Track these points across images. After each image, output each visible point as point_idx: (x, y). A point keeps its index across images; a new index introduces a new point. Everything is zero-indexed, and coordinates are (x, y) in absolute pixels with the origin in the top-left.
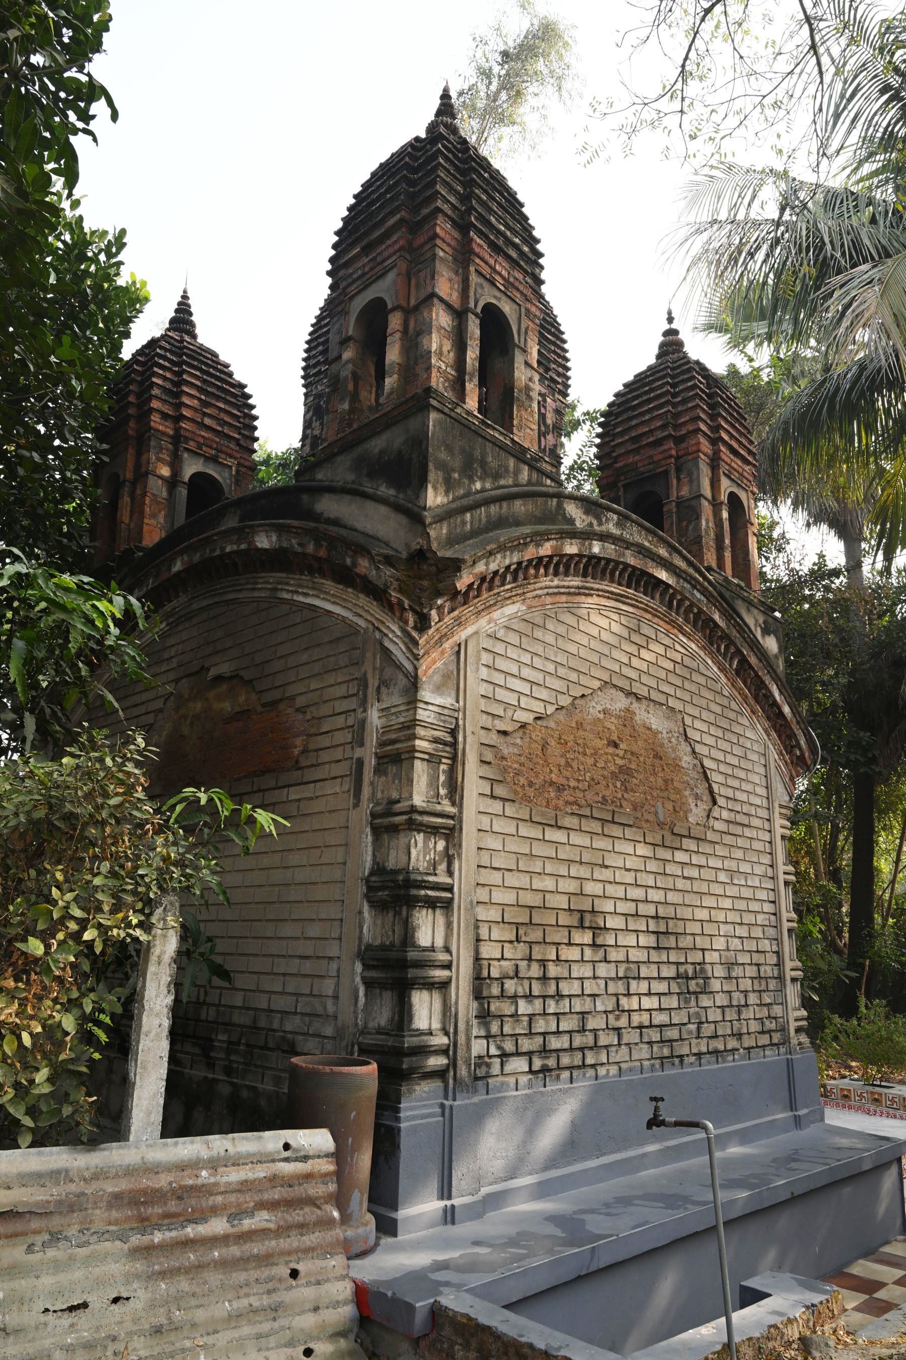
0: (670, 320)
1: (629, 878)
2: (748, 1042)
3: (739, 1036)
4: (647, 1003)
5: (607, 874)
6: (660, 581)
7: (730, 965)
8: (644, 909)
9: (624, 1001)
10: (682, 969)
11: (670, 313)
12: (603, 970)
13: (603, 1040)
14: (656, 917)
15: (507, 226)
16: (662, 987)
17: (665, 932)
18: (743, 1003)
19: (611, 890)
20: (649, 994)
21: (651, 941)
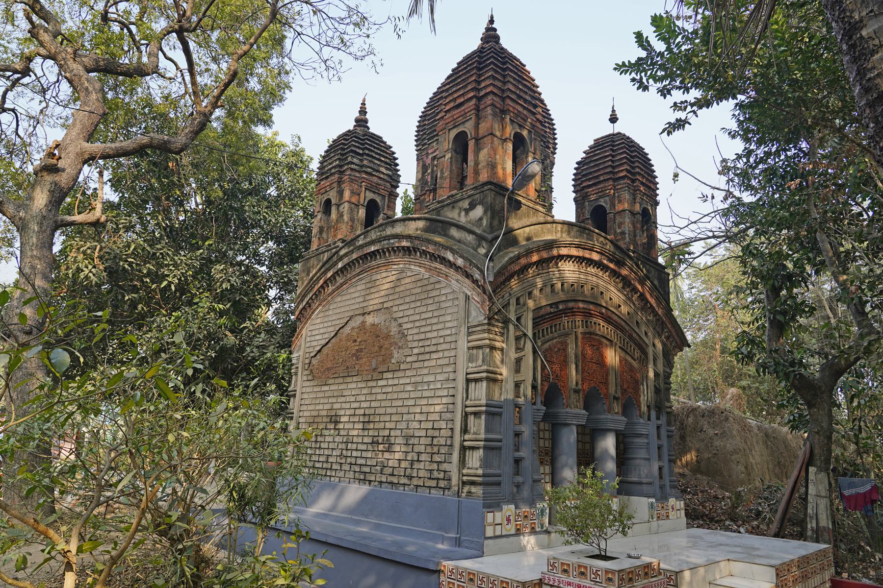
0: (492, 21)
1: (353, 399)
2: (415, 482)
3: (410, 478)
4: (355, 454)
5: (343, 399)
7: (407, 437)
8: (358, 412)
9: (344, 452)
10: (375, 439)
11: (492, 17)
12: (337, 439)
13: (334, 467)
14: (364, 415)
16: (364, 447)
17: (367, 421)
18: (416, 459)
19: (344, 405)
20: (356, 450)
21: (360, 426)
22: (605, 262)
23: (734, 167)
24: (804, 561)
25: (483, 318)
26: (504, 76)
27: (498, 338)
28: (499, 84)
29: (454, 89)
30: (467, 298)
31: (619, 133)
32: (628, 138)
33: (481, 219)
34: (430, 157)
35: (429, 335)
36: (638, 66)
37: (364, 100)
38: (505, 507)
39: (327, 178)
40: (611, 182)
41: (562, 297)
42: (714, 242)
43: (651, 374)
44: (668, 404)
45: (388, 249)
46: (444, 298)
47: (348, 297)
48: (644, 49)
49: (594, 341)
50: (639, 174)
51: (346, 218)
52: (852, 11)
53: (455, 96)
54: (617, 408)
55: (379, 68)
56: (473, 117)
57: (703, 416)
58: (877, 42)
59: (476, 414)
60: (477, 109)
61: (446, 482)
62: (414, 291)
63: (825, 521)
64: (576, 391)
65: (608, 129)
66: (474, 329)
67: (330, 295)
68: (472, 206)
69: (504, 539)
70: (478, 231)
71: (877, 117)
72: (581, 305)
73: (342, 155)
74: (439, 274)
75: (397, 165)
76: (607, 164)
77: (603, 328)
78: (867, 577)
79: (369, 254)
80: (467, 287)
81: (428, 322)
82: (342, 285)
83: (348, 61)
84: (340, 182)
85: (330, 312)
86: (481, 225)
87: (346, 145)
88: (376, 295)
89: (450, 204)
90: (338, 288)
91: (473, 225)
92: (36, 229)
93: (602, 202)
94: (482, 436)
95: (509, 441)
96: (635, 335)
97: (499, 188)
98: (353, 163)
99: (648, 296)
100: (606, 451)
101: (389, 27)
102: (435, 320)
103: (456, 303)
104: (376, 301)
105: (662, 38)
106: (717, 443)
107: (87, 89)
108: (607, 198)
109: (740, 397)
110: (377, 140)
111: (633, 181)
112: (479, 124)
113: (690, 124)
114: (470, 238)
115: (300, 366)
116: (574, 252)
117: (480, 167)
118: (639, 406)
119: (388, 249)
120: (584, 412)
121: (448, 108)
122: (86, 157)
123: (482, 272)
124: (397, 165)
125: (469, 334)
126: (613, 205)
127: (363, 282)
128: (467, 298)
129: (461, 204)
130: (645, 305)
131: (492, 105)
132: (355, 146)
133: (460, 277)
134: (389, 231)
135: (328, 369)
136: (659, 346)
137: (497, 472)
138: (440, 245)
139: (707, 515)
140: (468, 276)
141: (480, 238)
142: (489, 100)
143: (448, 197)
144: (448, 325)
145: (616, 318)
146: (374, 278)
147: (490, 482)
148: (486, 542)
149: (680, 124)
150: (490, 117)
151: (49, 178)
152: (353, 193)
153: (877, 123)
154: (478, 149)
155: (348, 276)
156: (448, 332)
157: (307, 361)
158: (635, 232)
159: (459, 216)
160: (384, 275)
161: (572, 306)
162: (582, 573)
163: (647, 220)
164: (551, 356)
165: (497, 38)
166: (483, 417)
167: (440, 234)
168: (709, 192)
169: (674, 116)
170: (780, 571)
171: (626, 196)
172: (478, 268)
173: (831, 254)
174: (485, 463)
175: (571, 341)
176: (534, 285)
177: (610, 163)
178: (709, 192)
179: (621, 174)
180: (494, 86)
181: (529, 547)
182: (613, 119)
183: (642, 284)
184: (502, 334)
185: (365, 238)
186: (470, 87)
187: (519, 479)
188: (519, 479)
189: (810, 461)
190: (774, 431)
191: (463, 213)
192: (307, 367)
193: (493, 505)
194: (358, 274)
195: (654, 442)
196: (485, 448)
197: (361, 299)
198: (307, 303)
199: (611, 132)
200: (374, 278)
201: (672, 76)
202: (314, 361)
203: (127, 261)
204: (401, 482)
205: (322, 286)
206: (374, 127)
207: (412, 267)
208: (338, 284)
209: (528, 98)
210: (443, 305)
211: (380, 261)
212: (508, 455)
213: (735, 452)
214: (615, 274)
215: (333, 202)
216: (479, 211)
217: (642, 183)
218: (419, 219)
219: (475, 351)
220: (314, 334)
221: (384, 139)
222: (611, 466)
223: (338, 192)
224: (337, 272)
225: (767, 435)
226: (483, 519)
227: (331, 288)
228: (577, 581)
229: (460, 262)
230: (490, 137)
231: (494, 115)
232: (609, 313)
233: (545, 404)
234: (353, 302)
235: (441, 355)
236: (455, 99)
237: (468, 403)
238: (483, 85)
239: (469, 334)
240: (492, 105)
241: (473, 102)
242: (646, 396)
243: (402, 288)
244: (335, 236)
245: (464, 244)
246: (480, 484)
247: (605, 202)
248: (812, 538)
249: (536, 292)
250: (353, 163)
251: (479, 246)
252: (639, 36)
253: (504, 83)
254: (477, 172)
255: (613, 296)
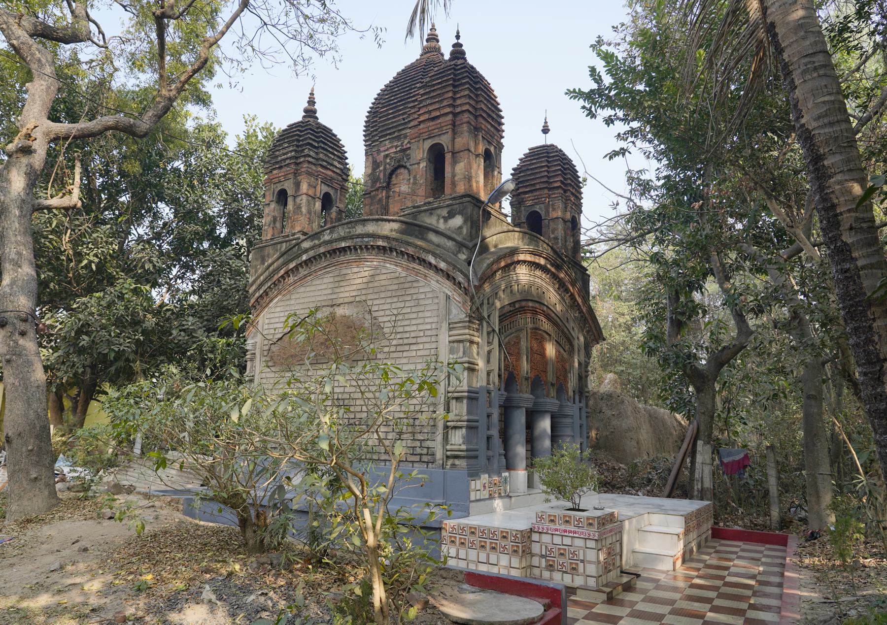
0: (458, 37)
6: (343, 248)
10: (352, 421)
11: (458, 33)
15: (284, 154)
22: (549, 266)
23: (638, 178)
24: (699, 512)
25: (464, 316)
26: (477, 96)
27: (475, 333)
28: (472, 102)
29: (428, 102)
30: (448, 297)
31: (552, 145)
32: (561, 151)
33: (460, 228)
34: (383, 154)
35: (407, 329)
36: (589, 96)
37: (313, 90)
38: (482, 476)
39: (281, 167)
40: (546, 191)
41: (518, 297)
42: (616, 243)
43: (576, 365)
44: (586, 390)
45: (360, 247)
46: (423, 296)
47: (313, 288)
48: (596, 81)
49: (539, 337)
50: (571, 185)
51: (304, 210)
52: (819, 147)
53: (431, 108)
54: (553, 393)
55: (338, 64)
56: (450, 131)
57: (602, 399)
58: (833, 171)
59: (457, 399)
60: (454, 125)
61: (429, 457)
62: (391, 288)
63: (708, 484)
64: (527, 379)
65: (540, 140)
66: (455, 325)
67: (290, 285)
68: (451, 215)
69: (482, 502)
70: (459, 239)
71: (829, 218)
72: (530, 304)
73: (297, 146)
74: (417, 273)
75: (347, 158)
76: (543, 174)
77: (546, 325)
78: (738, 525)
79: (338, 249)
80: (447, 288)
81: (407, 316)
82: (305, 276)
83: (315, 55)
84: (296, 174)
85: (292, 302)
86: (461, 233)
87: (300, 136)
88: (347, 289)
89: (427, 210)
90: (301, 279)
91: (453, 232)
92: (17, 213)
93: (537, 208)
94: (466, 418)
95: (483, 422)
96: (565, 330)
97: (476, 201)
98: (310, 156)
99: (577, 297)
100: (545, 430)
101: (371, 35)
102: (414, 316)
103: (436, 301)
104: (347, 295)
105: (609, 72)
106: (614, 423)
107: (39, 61)
108: (542, 206)
109: (616, 381)
110: (327, 132)
111: (565, 191)
112: (454, 138)
113: (629, 152)
114: (450, 244)
115: (258, 352)
116: (529, 258)
117: (456, 178)
118: (567, 392)
119: (360, 247)
120: (531, 396)
121: (422, 118)
122: (52, 137)
123: (467, 276)
124: (347, 158)
125: (450, 329)
126: (547, 212)
127: (330, 275)
128: (448, 297)
129: (439, 211)
130: (574, 305)
131: (469, 122)
132: (311, 139)
133: (439, 279)
134: (359, 230)
135: (292, 356)
136: (582, 339)
137: (475, 447)
138: (421, 248)
139: (609, 483)
140: (448, 277)
141: (461, 245)
142: (466, 117)
143: (425, 204)
144: (427, 320)
145: (553, 315)
146: (344, 272)
147: (471, 456)
148: (472, 505)
149: (623, 152)
150: (466, 134)
151: (24, 160)
152: (310, 185)
153: (829, 222)
154: (455, 162)
155: (313, 268)
156: (429, 327)
157: (266, 348)
158: (565, 238)
159: (438, 222)
160: (356, 270)
161: (526, 305)
162: (567, 522)
163: (574, 225)
164: (510, 349)
165: (463, 53)
166: (465, 401)
167: (417, 237)
168: (615, 199)
169: (619, 145)
170: (688, 518)
171: (560, 204)
172: (462, 273)
173: (718, 265)
174: (467, 440)
175: (523, 335)
176: (499, 287)
177: (546, 173)
178: (615, 199)
179: (556, 185)
180: (470, 105)
181: (498, 510)
182: (546, 130)
183: (573, 285)
184: (478, 330)
185: (331, 233)
186: (445, 103)
187: (490, 453)
188: (490, 453)
189: (696, 438)
190: (655, 412)
191: (442, 221)
192: (266, 353)
193: (474, 474)
194: (325, 267)
195: (577, 422)
196: (468, 427)
197: (329, 291)
198: (265, 291)
199: (542, 143)
200: (344, 272)
201: (612, 104)
202: (274, 348)
203: (47, 238)
204: (382, 458)
205: (282, 276)
206: (324, 118)
207: (388, 265)
208: (301, 275)
209: (495, 116)
210: (422, 302)
211: (349, 257)
212: (483, 433)
213: (630, 430)
214: (554, 276)
215: (289, 192)
216: (458, 221)
217: (572, 194)
218: (393, 221)
219: (455, 345)
220: (270, 321)
221: (334, 132)
222: (547, 443)
223: (294, 183)
224: (300, 264)
225: (650, 416)
226: (469, 486)
227: (292, 279)
228: (563, 527)
229: (442, 265)
230: (467, 152)
231: (470, 132)
232: (549, 312)
233: (506, 389)
234: (320, 293)
235: (421, 346)
236: (430, 112)
237: (450, 389)
238: (458, 102)
239: (450, 329)
240: (469, 122)
241: (450, 117)
242: (572, 383)
243: (376, 284)
244: (293, 227)
245: (443, 248)
246: (464, 457)
247: (540, 209)
248: (697, 496)
249: (501, 294)
250: (310, 156)
251: (459, 252)
252: (593, 70)
253: (477, 102)
254: (454, 184)
255: (552, 296)
